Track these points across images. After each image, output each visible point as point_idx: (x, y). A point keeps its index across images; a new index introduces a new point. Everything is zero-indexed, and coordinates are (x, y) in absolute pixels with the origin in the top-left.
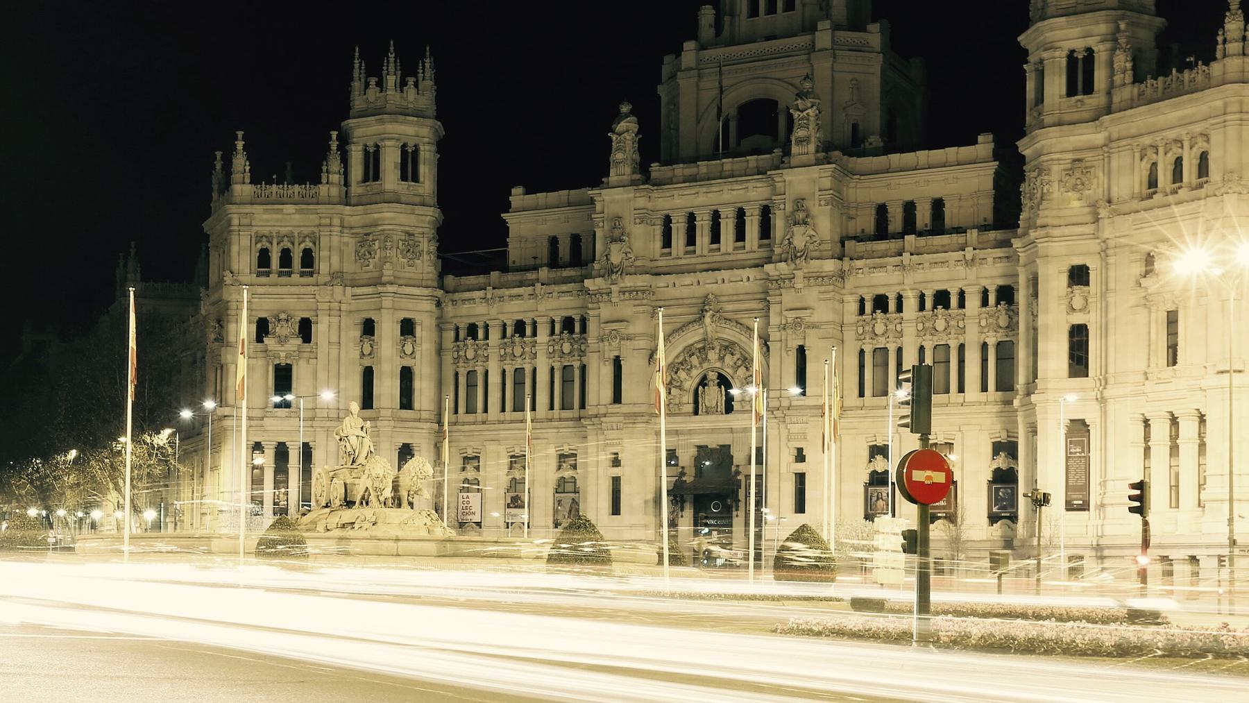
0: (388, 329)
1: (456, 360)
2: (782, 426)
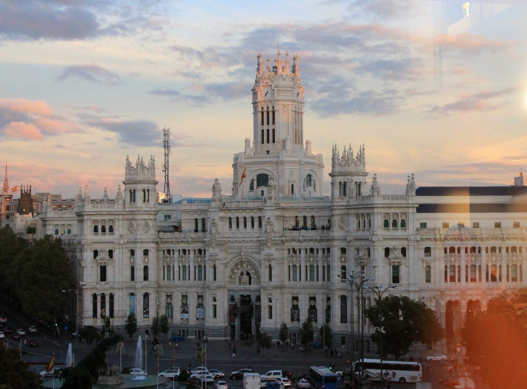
0: (139, 253)
1: (163, 262)
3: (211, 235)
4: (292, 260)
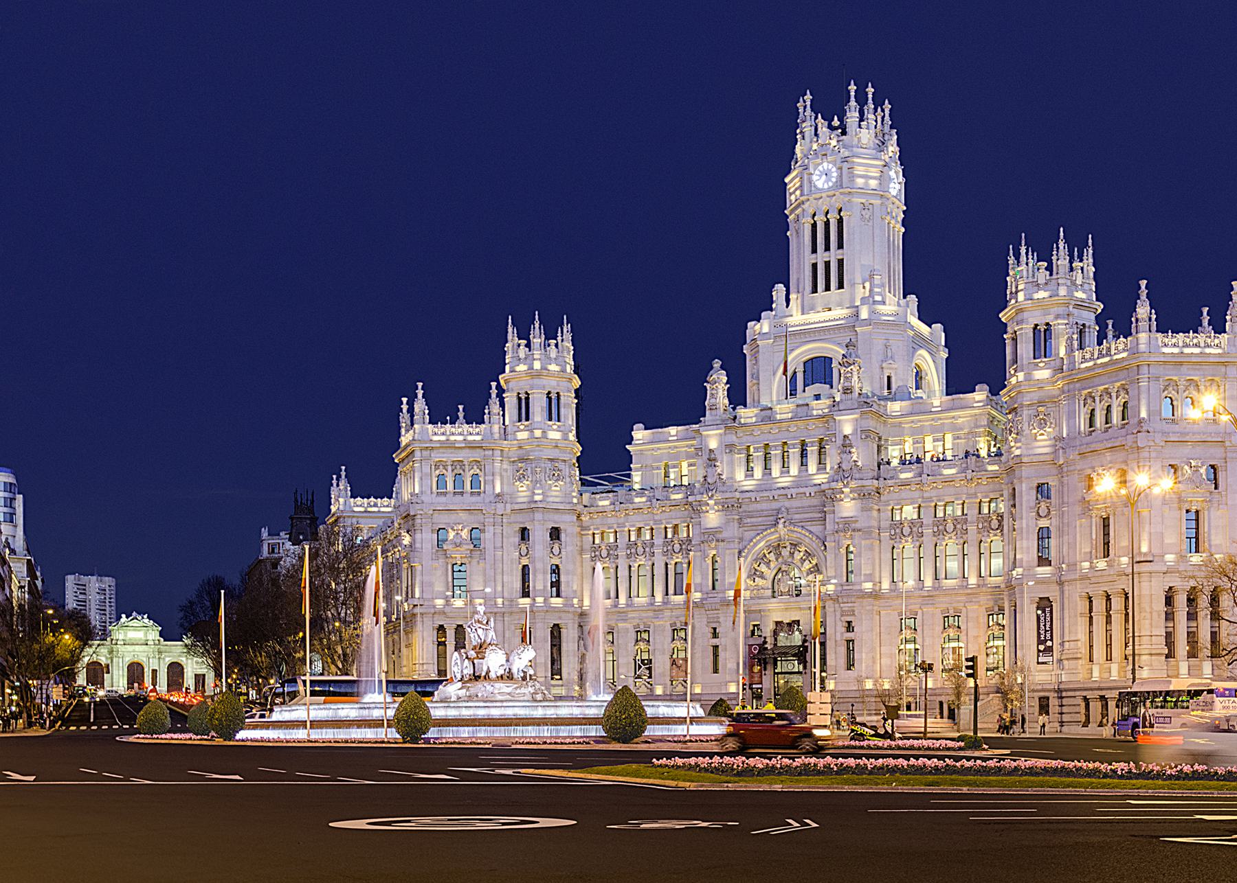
0: (540, 535)
2: (837, 605)
3: (706, 486)
4: (902, 532)
